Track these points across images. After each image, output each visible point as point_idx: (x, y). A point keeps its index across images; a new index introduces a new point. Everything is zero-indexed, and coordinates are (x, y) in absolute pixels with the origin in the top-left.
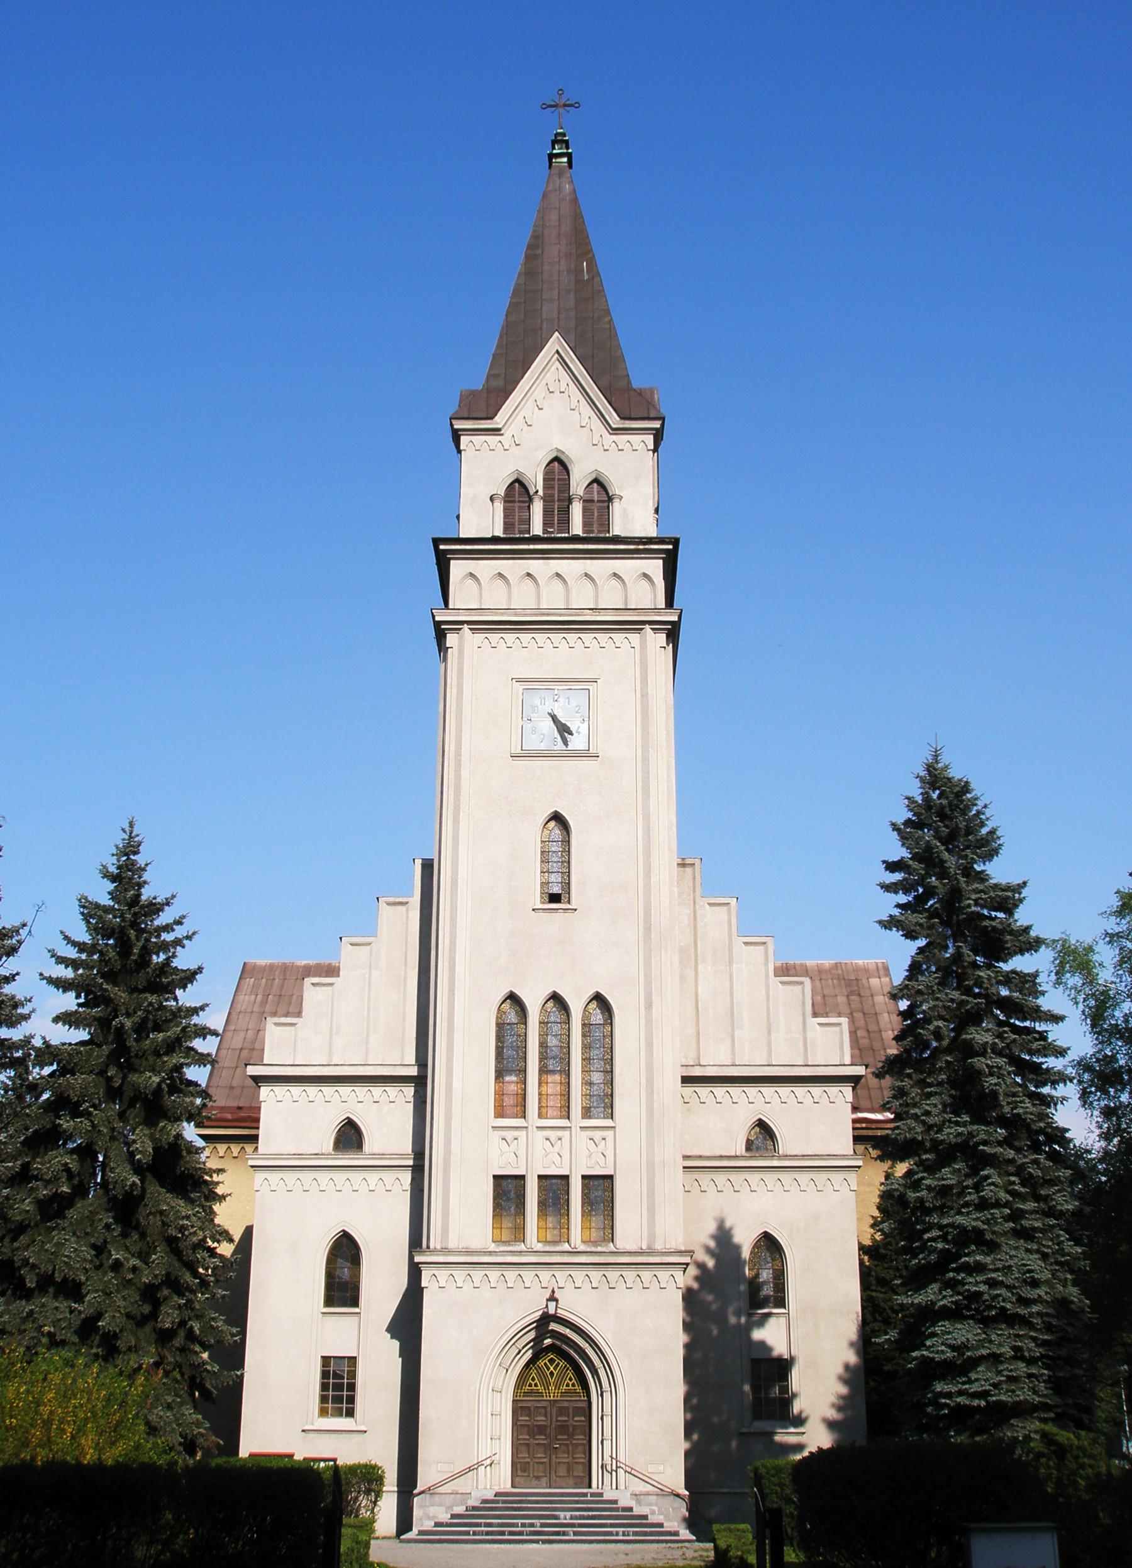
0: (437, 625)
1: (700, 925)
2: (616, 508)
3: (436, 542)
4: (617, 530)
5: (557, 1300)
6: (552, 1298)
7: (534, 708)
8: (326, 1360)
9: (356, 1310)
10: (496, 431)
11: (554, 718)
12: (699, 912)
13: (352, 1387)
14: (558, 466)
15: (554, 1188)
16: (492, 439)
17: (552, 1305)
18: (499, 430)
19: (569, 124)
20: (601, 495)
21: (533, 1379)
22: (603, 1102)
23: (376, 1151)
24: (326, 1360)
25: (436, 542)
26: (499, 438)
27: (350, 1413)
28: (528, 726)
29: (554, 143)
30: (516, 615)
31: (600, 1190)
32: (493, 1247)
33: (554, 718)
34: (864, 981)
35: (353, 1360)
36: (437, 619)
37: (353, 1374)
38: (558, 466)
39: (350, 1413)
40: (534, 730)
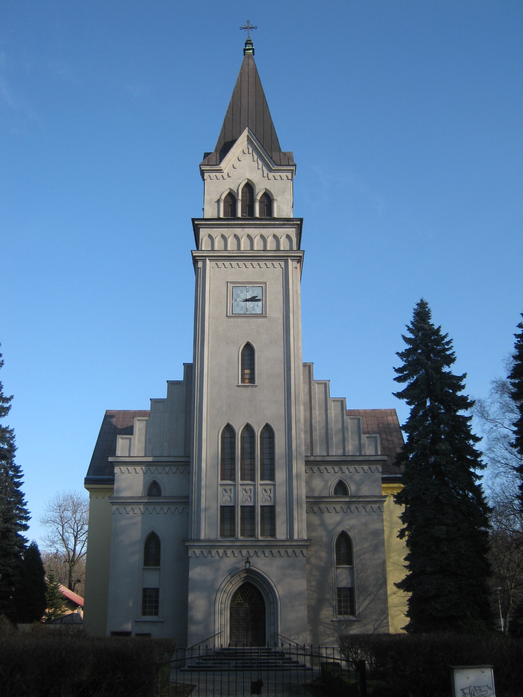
0: (194, 257)
1: (312, 392)
2: (275, 205)
3: (193, 220)
4: (275, 215)
5: (249, 562)
6: (248, 562)
7: (238, 296)
8: (145, 590)
9: (159, 567)
10: (220, 171)
11: (247, 300)
12: (312, 387)
13: (157, 602)
14: (249, 187)
15: (249, 512)
16: (219, 175)
17: (248, 565)
18: (222, 170)
19: (253, 36)
20: (268, 199)
21: (239, 598)
22: (269, 474)
23: (167, 495)
24: (145, 590)
25: (193, 220)
26: (222, 174)
27: (156, 614)
28: (235, 304)
29: (246, 44)
30: (229, 253)
31: (269, 512)
32: (219, 538)
33: (247, 300)
34: (385, 418)
35: (157, 590)
36: (194, 255)
37: (157, 596)
38: (249, 187)
39: (156, 614)
40: (238, 305)
